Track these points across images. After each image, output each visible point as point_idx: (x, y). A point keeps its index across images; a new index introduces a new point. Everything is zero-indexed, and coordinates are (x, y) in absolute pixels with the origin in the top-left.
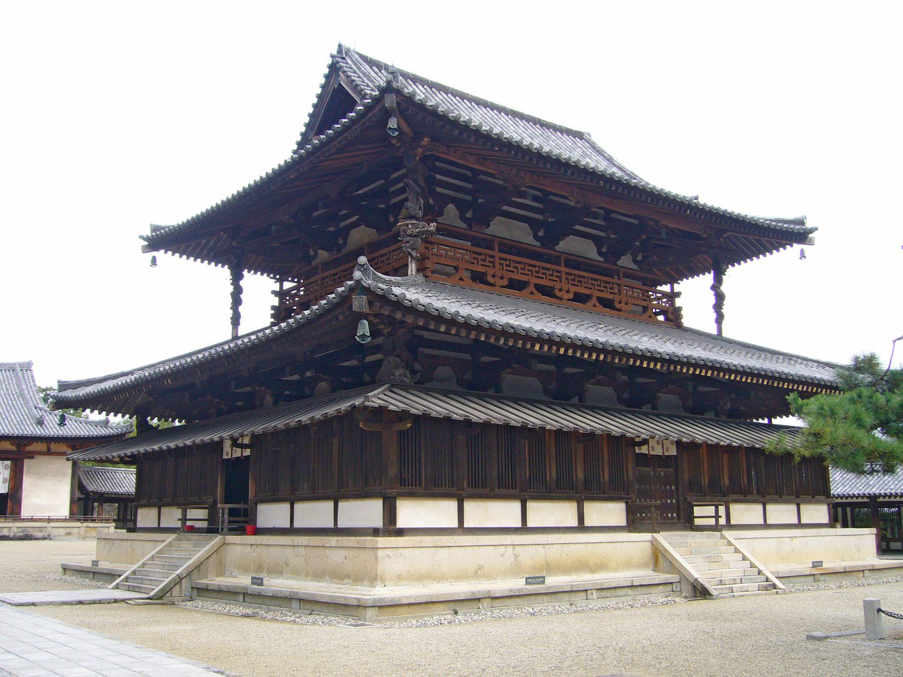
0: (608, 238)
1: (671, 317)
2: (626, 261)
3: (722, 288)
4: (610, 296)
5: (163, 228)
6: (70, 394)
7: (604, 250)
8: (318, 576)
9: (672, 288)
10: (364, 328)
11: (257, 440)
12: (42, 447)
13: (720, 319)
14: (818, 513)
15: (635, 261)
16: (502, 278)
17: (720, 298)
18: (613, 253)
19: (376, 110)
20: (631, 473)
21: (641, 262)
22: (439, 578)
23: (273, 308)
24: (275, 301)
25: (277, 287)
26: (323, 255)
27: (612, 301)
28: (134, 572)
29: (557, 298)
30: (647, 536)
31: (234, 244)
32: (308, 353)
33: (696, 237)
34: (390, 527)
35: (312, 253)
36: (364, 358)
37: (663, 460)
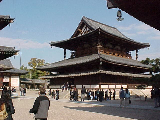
2: (124, 49)
9: (130, 53)
10: (101, 63)
12: (14, 74)
15: (125, 49)
17: (137, 55)
18: (122, 48)
24: (71, 54)
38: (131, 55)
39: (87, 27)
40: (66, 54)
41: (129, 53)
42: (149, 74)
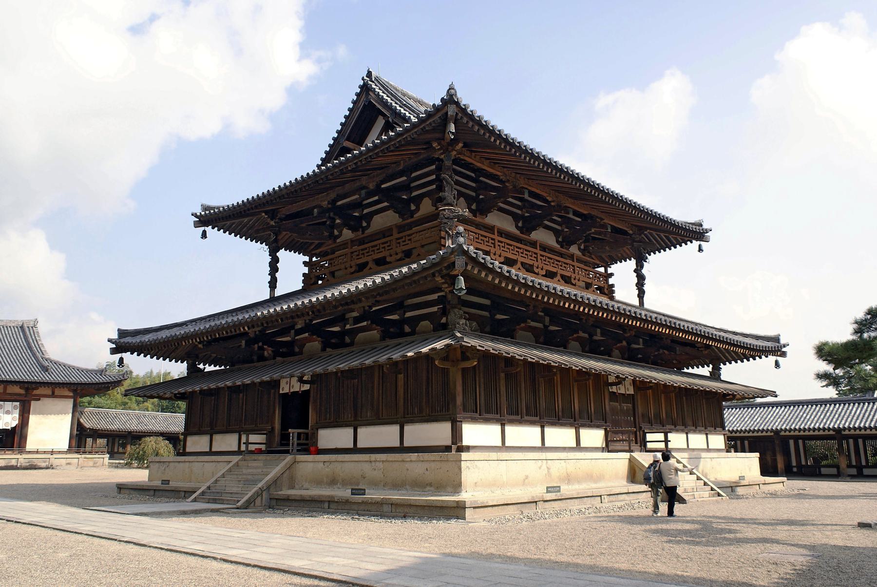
0: (563, 231)
1: (606, 291)
2: (574, 250)
3: (644, 271)
4: (568, 274)
5: (213, 208)
6: (129, 340)
7: (560, 240)
8: (397, 486)
9: (606, 270)
11: (316, 379)
12: (48, 391)
13: (641, 294)
14: (718, 441)
15: (579, 249)
16: (500, 256)
18: (566, 242)
19: (436, 117)
20: (607, 407)
21: (584, 250)
23: (304, 275)
24: (306, 270)
25: (307, 259)
26: (347, 234)
27: (570, 278)
28: (209, 488)
29: (535, 273)
30: (627, 455)
31: (272, 223)
32: (367, 308)
33: (625, 233)
34: (457, 446)
35: (336, 232)
36: (404, 313)
37: (625, 397)
38: (611, 281)
40: (277, 270)
41: (602, 270)
42: (708, 374)
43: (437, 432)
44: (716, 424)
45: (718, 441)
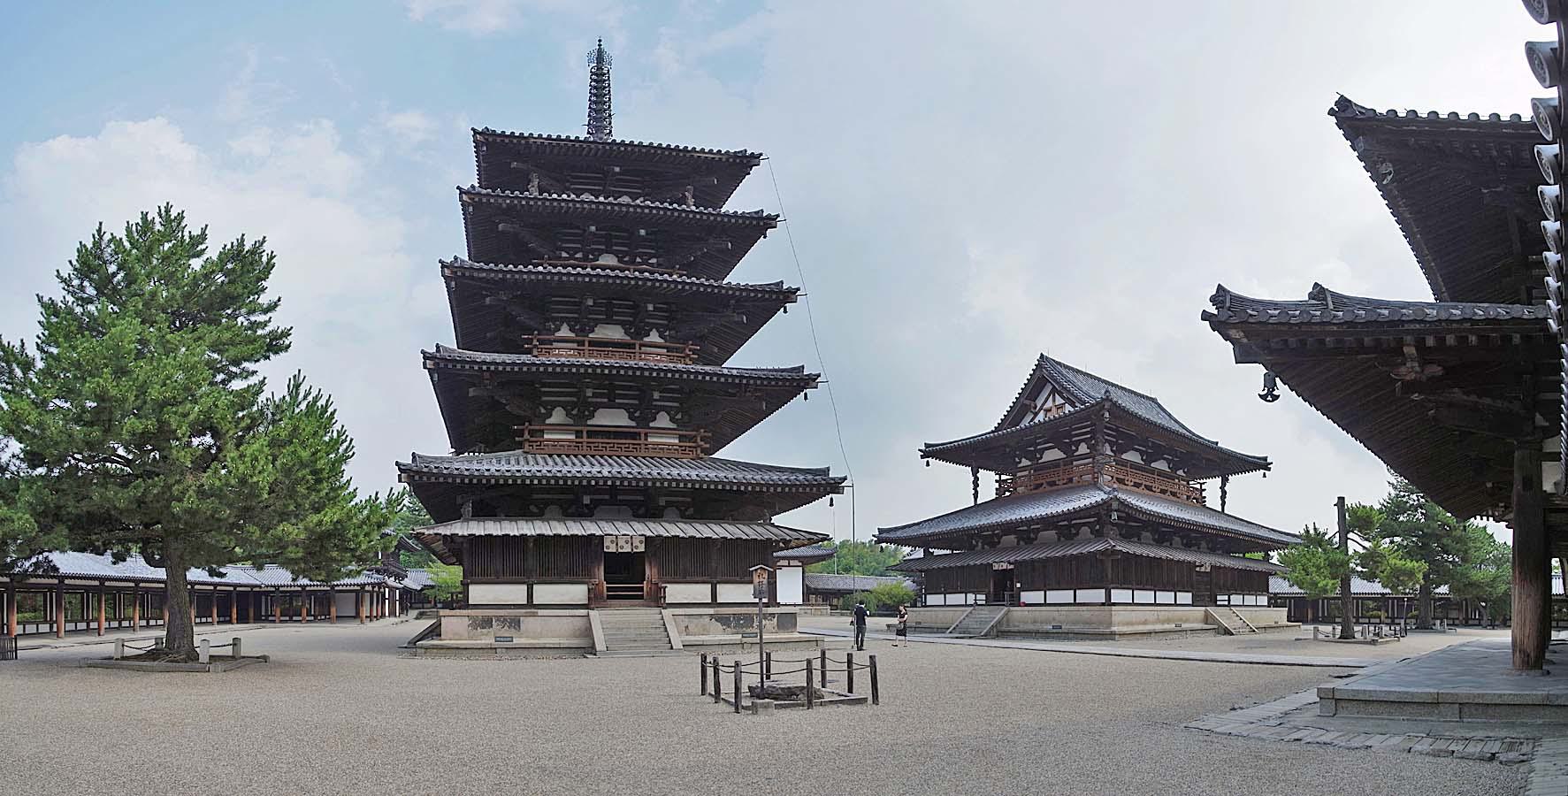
2: (1180, 472)
14: (1263, 600)
22: (1132, 624)
26: (1025, 462)
34: (1108, 603)
39: (1054, 391)
43: (1098, 595)
44: (1264, 589)
45: (1263, 600)
